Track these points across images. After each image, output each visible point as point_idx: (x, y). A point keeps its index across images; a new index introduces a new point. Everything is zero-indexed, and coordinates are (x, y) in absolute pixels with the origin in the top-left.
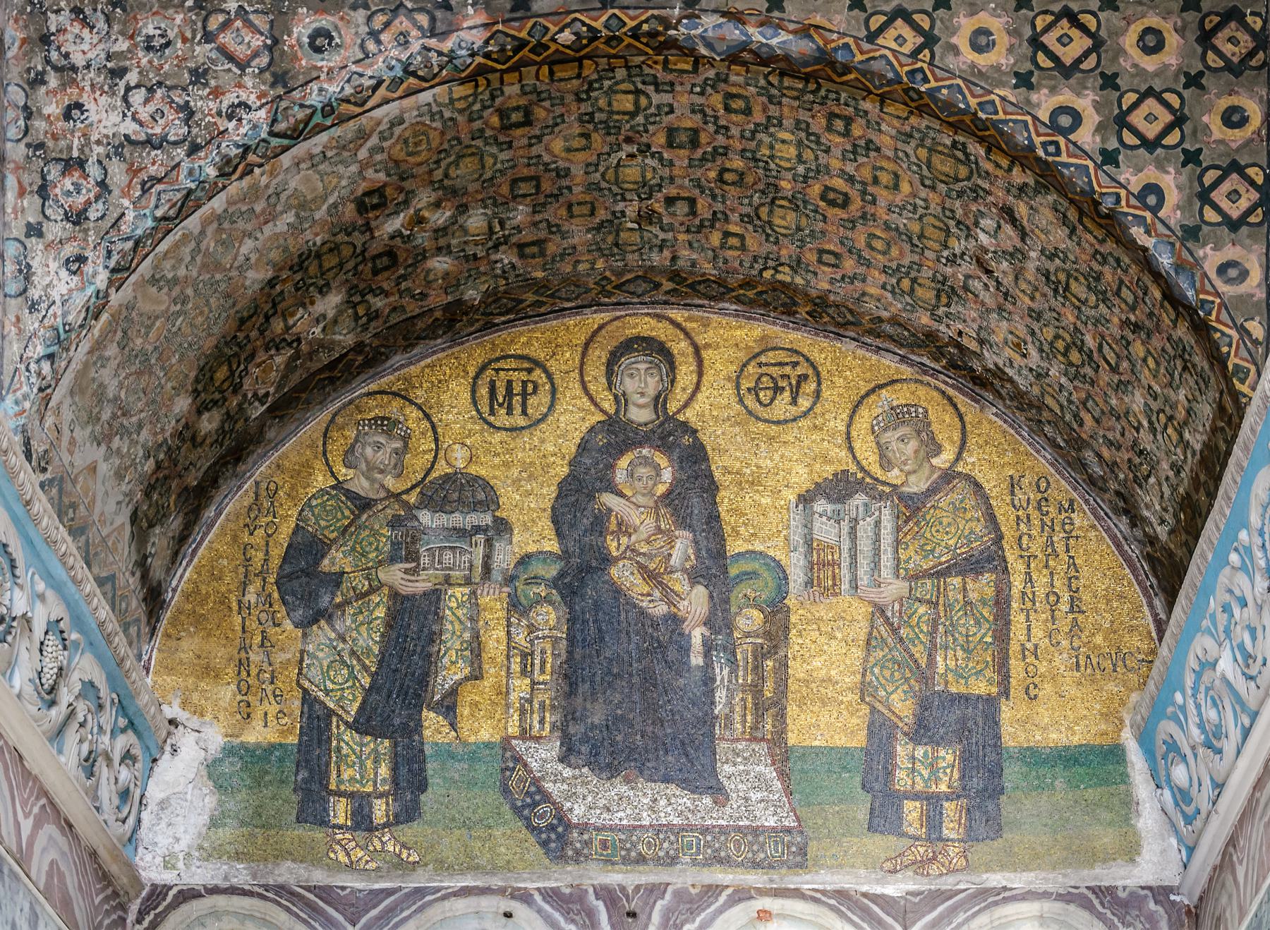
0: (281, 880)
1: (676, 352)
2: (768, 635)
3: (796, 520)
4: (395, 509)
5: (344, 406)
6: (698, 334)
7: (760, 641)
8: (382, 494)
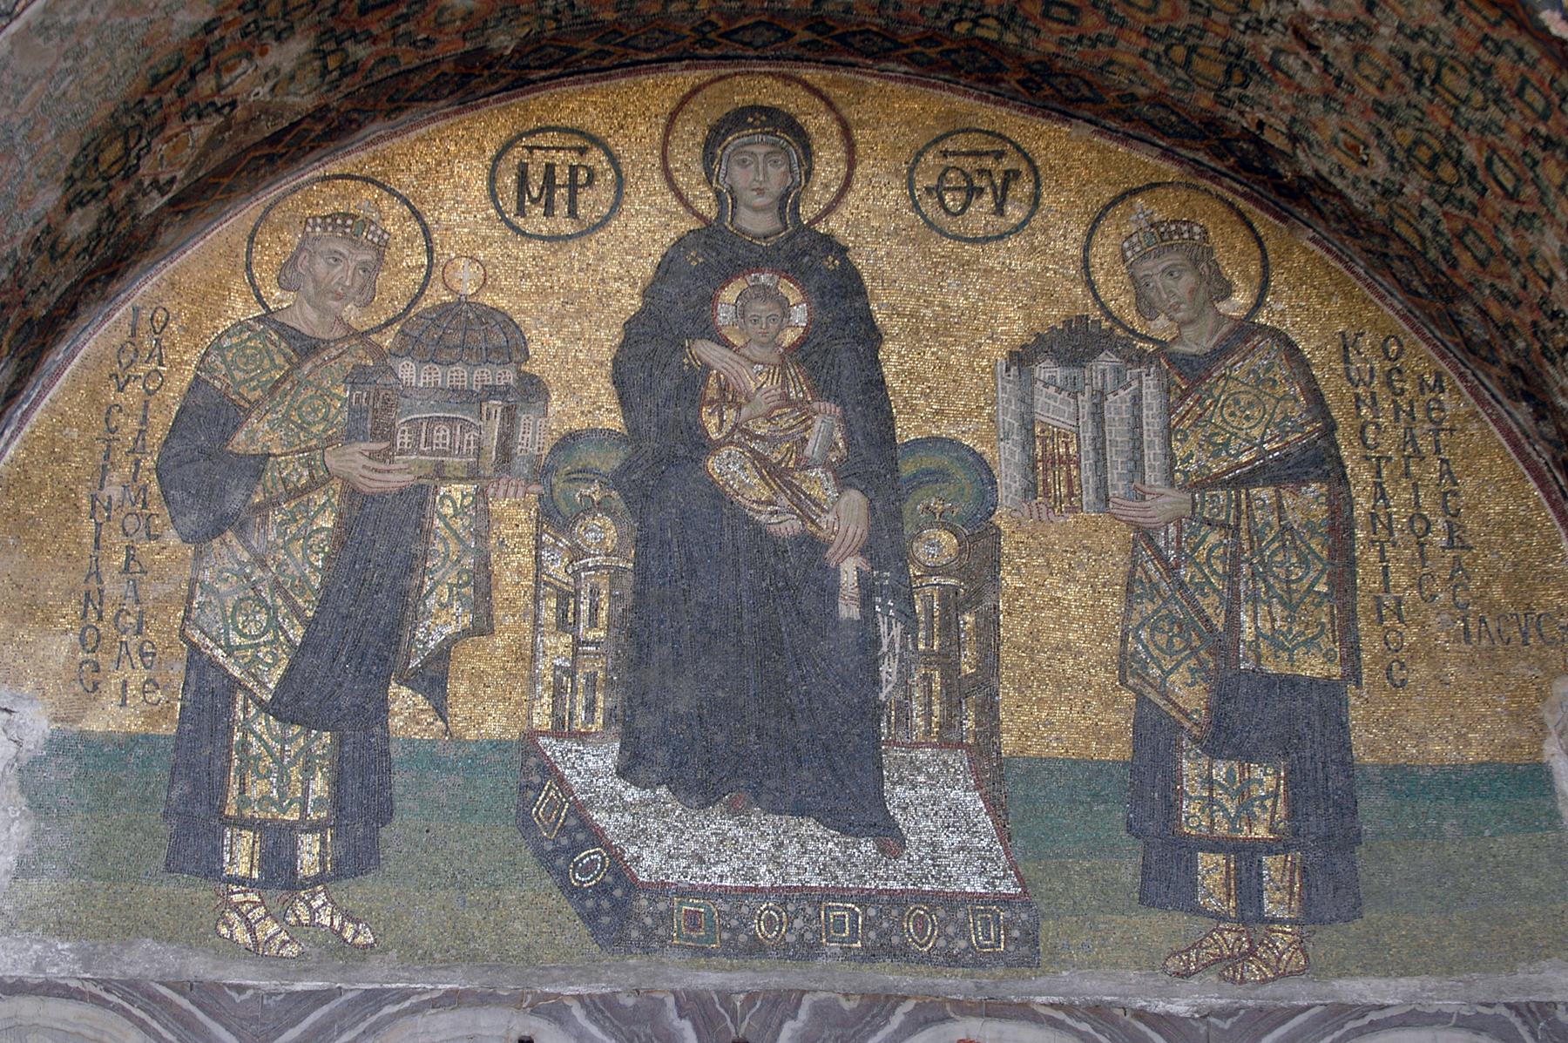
0: (133, 972)
1: (812, 130)
2: (963, 572)
3: (1007, 393)
4: (360, 356)
5: (284, 196)
6: (850, 104)
7: (952, 582)
8: (339, 333)
